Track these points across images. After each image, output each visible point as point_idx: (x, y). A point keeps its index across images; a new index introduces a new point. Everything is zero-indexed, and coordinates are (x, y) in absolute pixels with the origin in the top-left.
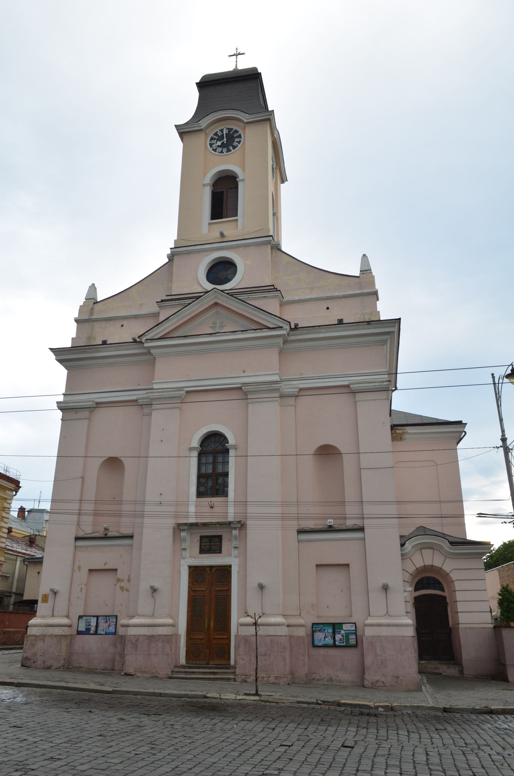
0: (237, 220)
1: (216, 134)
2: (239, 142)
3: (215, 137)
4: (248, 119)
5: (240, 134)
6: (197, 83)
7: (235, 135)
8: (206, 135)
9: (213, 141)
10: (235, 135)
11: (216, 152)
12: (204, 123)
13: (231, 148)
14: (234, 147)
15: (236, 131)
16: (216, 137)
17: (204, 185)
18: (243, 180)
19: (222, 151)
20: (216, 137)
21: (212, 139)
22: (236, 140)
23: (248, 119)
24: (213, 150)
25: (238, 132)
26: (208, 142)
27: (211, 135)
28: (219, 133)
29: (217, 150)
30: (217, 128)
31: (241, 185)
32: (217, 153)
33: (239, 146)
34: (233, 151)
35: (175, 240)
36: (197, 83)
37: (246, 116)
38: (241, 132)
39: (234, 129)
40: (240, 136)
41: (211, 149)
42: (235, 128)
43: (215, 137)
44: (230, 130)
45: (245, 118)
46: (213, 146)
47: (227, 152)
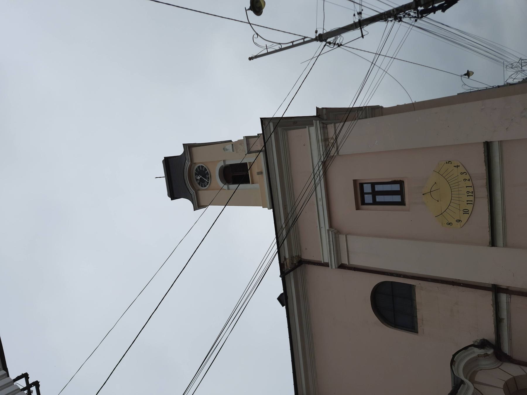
1: (199, 184)
2: (202, 167)
4: (189, 162)
6: (172, 200)
8: (199, 190)
11: (209, 182)
12: (192, 191)
17: (228, 189)
18: (224, 161)
19: (208, 178)
21: (202, 186)
22: (201, 169)
23: (189, 162)
24: (207, 185)
25: (197, 168)
27: (200, 187)
30: (196, 183)
31: (228, 163)
33: (205, 167)
34: (208, 171)
36: (172, 200)
37: (187, 163)
38: (196, 167)
40: (199, 167)
42: (194, 171)
44: (196, 174)
45: (188, 163)
46: (206, 185)
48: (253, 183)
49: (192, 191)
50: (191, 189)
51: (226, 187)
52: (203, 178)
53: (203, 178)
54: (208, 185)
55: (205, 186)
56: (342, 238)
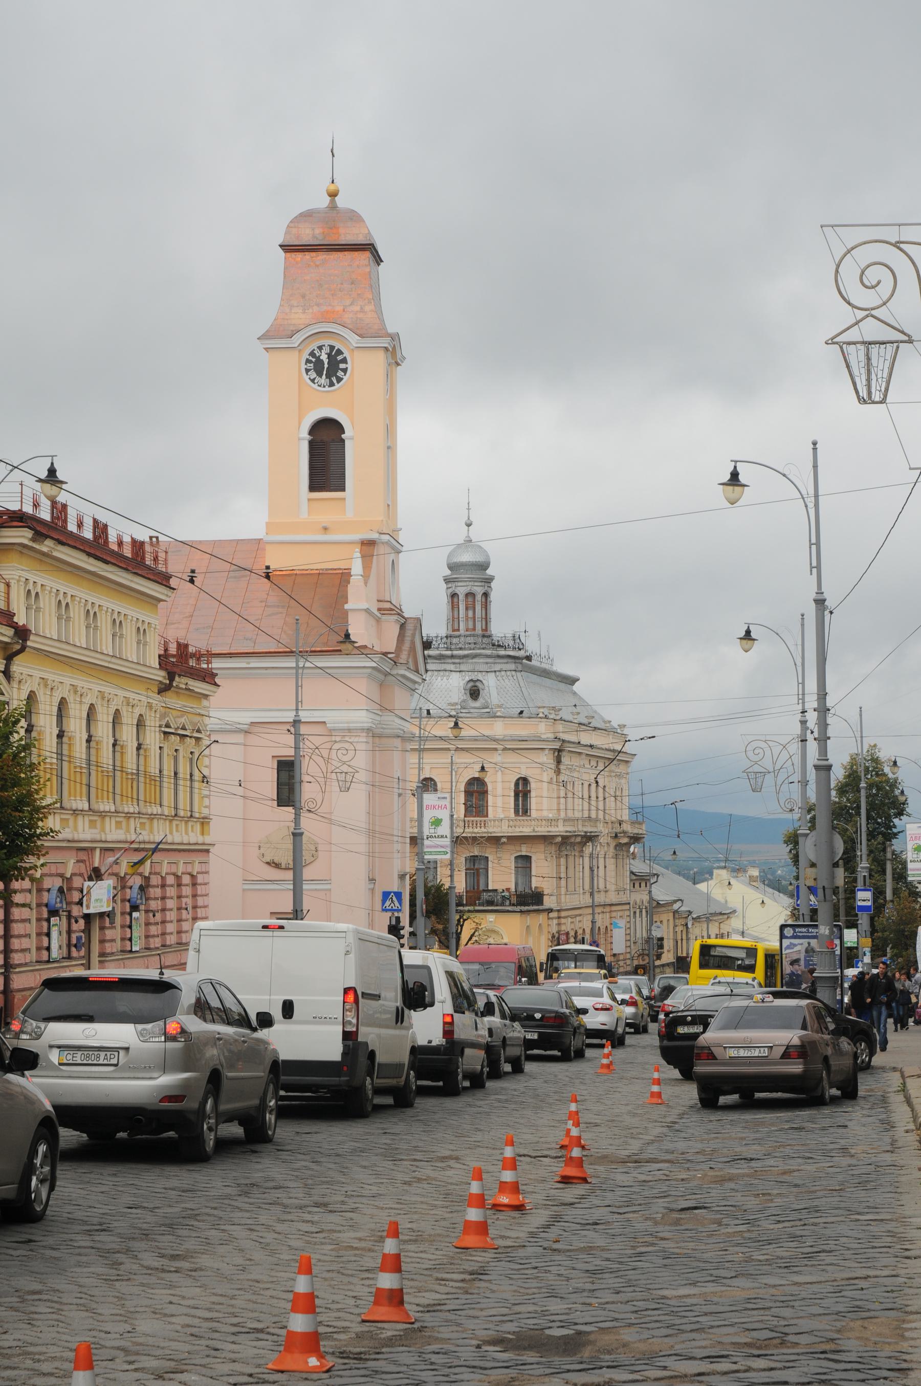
0: (345, 499)
2: (345, 371)
3: (311, 358)
4: (357, 343)
5: (345, 358)
7: (339, 358)
8: (300, 351)
9: (309, 365)
10: (339, 358)
13: (334, 379)
14: (339, 380)
15: (339, 352)
16: (314, 360)
17: (299, 439)
18: (351, 438)
20: (314, 360)
21: (308, 361)
22: (342, 366)
25: (343, 353)
26: (304, 367)
27: (306, 355)
28: (316, 352)
29: (316, 381)
30: (314, 346)
32: (315, 386)
33: (345, 378)
35: (267, 523)
38: (346, 354)
39: (336, 348)
40: (344, 361)
41: (306, 378)
42: (338, 346)
43: (311, 358)
45: (354, 339)
47: (329, 386)
48: (309, 500)
49: (298, 339)
50: (302, 336)
51: (304, 434)
52: (325, 372)
53: (325, 372)
54: (309, 381)
55: (307, 371)
56: (239, 738)
